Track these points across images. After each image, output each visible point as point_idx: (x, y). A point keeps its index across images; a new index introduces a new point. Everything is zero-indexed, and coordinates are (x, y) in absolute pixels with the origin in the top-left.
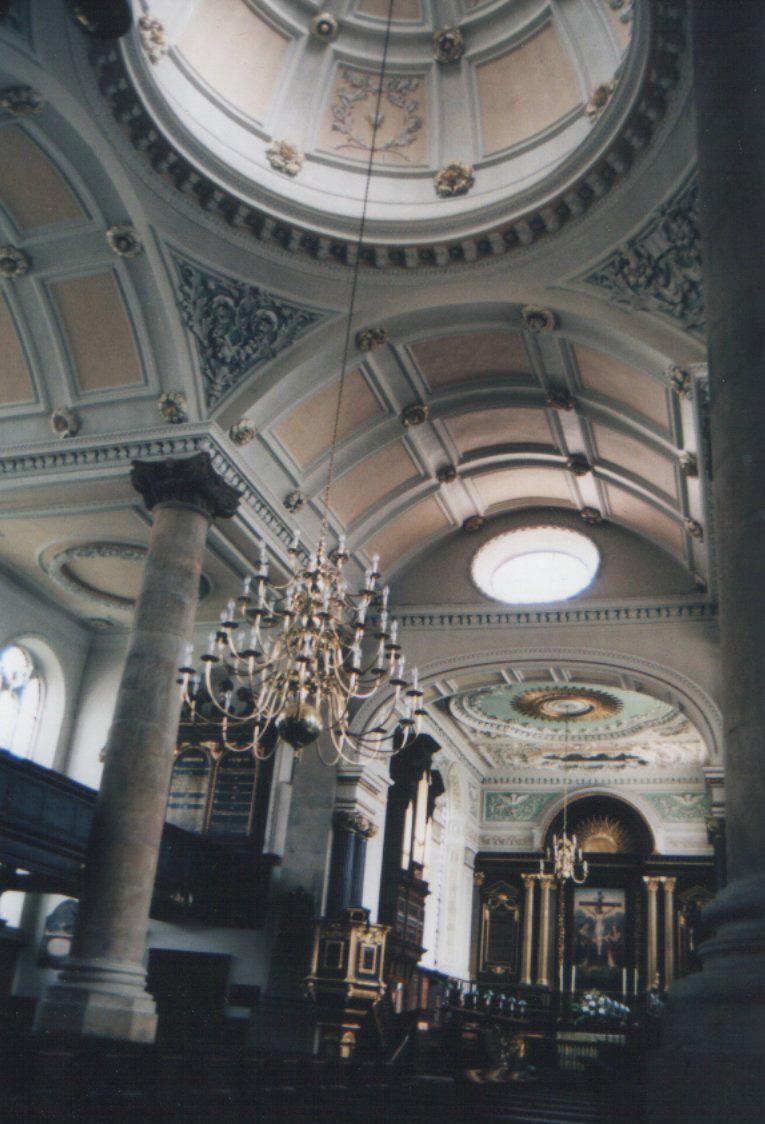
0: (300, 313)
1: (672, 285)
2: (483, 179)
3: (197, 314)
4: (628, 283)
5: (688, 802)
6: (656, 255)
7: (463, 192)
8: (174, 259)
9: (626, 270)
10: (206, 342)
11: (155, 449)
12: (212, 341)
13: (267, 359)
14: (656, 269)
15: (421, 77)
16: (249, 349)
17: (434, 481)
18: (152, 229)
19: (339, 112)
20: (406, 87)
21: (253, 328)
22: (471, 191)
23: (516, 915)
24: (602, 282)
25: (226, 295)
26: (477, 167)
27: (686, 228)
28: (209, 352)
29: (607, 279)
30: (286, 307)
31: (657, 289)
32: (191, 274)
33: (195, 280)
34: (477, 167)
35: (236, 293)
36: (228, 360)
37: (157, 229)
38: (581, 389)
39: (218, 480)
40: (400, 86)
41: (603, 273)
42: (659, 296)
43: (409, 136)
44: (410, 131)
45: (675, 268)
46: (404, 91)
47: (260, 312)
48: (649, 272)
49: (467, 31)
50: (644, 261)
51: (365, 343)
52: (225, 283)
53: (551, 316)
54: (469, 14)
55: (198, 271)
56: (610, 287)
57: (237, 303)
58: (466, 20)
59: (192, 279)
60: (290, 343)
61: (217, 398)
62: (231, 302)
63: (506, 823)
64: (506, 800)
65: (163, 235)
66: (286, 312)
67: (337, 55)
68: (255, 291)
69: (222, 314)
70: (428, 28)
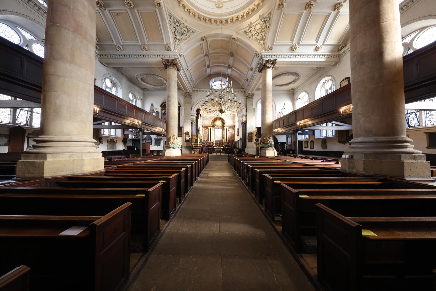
0: (191, 30)
3: (172, 27)
5: (230, 118)
10: (174, 34)
11: (166, 56)
12: (175, 34)
16: (182, 37)
17: (206, 68)
23: (208, 133)
24: (246, 33)
33: (172, 18)
39: (178, 64)
57: (180, 26)
59: (171, 18)
63: (206, 121)
64: (206, 118)
66: (189, 30)
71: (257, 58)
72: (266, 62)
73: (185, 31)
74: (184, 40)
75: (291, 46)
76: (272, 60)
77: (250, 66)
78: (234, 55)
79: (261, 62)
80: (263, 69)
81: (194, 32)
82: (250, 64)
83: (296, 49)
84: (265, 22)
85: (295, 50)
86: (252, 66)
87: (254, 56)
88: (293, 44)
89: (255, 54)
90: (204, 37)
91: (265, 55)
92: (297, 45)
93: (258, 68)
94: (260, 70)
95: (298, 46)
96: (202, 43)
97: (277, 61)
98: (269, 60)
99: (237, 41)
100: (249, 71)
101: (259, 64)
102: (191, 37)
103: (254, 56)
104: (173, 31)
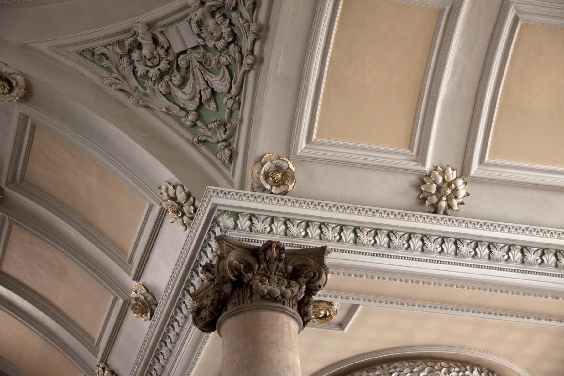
1: (188, 89)
4: (135, 73)
6: (177, 48)
9: (135, 55)
14: (173, 65)
24: (101, 60)
27: (225, 30)
29: (107, 58)
31: (168, 86)
41: (105, 50)
42: (168, 95)
48: (163, 65)
50: (162, 52)
53: (22, 83)
56: (108, 69)
72: (252, 260)
75: (413, 179)
76: (294, 253)
77: (137, 278)
79: (210, 255)
80: (230, 308)
82: (131, 261)
83: (455, 202)
84: (225, 16)
85: (443, 204)
86: (149, 277)
87: (163, 214)
88: (428, 167)
89: (165, 196)
91: (236, 216)
92: (452, 175)
93: (193, 296)
94: (204, 314)
95: (460, 182)
97: (329, 260)
98: (269, 245)
100: (131, 316)
101: (200, 269)
103: (163, 214)
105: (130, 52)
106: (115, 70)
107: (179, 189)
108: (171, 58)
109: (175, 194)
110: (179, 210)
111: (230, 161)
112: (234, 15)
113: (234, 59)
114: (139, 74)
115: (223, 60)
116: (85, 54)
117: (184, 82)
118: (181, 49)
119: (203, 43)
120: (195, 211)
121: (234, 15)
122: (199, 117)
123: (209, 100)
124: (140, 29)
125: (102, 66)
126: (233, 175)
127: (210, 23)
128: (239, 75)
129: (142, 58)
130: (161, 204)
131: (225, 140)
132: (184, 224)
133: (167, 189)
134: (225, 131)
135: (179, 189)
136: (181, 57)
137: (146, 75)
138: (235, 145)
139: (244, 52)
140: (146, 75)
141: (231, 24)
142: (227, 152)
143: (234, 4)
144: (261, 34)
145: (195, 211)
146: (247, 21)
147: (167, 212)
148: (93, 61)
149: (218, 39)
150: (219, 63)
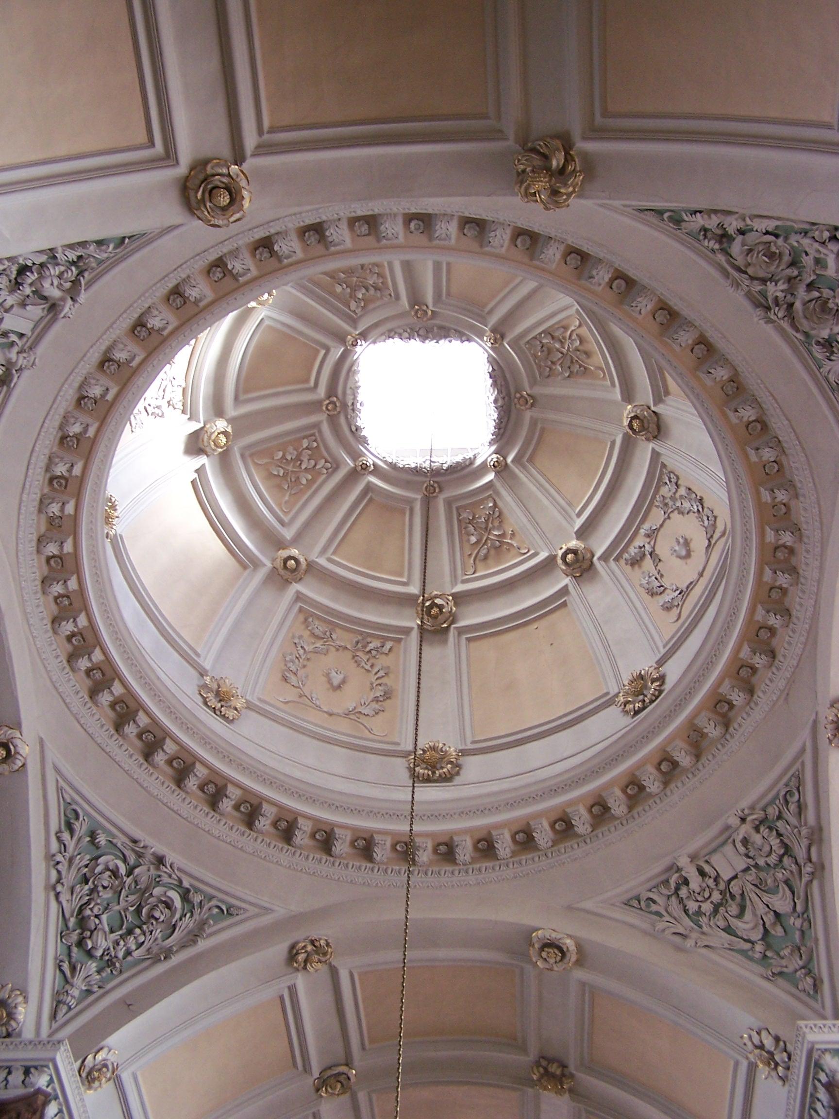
0: (214, 902)
1: (748, 915)
2: (473, 767)
3: (70, 877)
4: (686, 912)
6: (726, 875)
7: (447, 779)
8: (60, 790)
9: (683, 892)
10: (72, 922)
12: (82, 922)
13: (157, 960)
14: (727, 894)
15: (399, 641)
16: (131, 943)
18: (42, 742)
19: (292, 661)
20: (376, 649)
21: (144, 911)
22: (457, 780)
24: (648, 906)
25: (117, 857)
26: (464, 753)
27: (775, 842)
28: (75, 937)
29: (654, 902)
30: (197, 890)
32: (77, 817)
33: (81, 828)
34: (464, 753)
35: (132, 859)
36: (99, 953)
37: (48, 745)
38: (591, 1067)
40: (371, 646)
41: (651, 895)
43: (374, 705)
44: (376, 700)
45: (751, 893)
46: (374, 652)
47: (157, 891)
48: (716, 897)
49: (459, 599)
50: (711, 882)
51: (301, 957)
52: (121, 840)
54: (464, 582)
55: (87, 814)
56: (658, 914)
57: (129, 873)
58: (460, 588)
59: (77, 825)
60: (195, 942)
61: (70, 1008)
62: (123, 870)
65: (52, 754)
66: (197, 899)
67: (299, 597)
68: (160, 860)
69: (106, 884)
70: (414, 589)
71: (783, 1079)
73: (161, 906)
74: (148, 962)
78: (572, 1076)
81: (230, 914)
84: (770, 828)
87: (752, 1068)
89: (750, 1046)
90: (312, 942)
96: (292, 990)
99: (579, 963)
102: (202, 945)
103: (752, 1068)
104: (70, 905)
105: (677, 889)
106: (664, 913)
107: (764, 1034)
108: (722, 886)
109: (761, 1042)
110: (770, 1060)
111: (816, 991)
112: (780, 824)
113: (791, 872)
114: (690, 912)
115: (779, 876)
116: (631, 903)
117: (742, 909)
118: (733, 874)
119: (753, 863)
120: (789, 1058)
121: (780, 824)
122: (768, 946)
123: (774, 924)
124: (683, 861)
125: (650, 912)
126: (823, 1007)
127: (757, 838)
128: (800, 888)
129: (691, 893)
130: (747, 1058)
131: (803, 967)
132: (780, 1078)
133: (750, 1037)
134: (801, 956)
135: (764, 1034)
136: (733, 883)
137: (699, 913)
138: (816, 971)
139: (801, 861)
140: (699, 913)
141: (779, 835)
142: (809, 980)
143: (777, 813)
144: (815, 837)
145: (789, 1058)
146: (796, 827)
147: (757, 1066)
148: (641, 909)
149: (769, 854)
150: (775, 880)
